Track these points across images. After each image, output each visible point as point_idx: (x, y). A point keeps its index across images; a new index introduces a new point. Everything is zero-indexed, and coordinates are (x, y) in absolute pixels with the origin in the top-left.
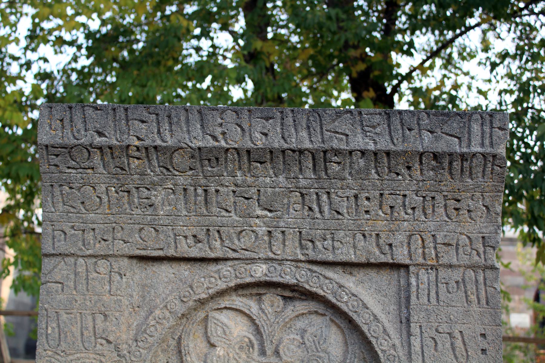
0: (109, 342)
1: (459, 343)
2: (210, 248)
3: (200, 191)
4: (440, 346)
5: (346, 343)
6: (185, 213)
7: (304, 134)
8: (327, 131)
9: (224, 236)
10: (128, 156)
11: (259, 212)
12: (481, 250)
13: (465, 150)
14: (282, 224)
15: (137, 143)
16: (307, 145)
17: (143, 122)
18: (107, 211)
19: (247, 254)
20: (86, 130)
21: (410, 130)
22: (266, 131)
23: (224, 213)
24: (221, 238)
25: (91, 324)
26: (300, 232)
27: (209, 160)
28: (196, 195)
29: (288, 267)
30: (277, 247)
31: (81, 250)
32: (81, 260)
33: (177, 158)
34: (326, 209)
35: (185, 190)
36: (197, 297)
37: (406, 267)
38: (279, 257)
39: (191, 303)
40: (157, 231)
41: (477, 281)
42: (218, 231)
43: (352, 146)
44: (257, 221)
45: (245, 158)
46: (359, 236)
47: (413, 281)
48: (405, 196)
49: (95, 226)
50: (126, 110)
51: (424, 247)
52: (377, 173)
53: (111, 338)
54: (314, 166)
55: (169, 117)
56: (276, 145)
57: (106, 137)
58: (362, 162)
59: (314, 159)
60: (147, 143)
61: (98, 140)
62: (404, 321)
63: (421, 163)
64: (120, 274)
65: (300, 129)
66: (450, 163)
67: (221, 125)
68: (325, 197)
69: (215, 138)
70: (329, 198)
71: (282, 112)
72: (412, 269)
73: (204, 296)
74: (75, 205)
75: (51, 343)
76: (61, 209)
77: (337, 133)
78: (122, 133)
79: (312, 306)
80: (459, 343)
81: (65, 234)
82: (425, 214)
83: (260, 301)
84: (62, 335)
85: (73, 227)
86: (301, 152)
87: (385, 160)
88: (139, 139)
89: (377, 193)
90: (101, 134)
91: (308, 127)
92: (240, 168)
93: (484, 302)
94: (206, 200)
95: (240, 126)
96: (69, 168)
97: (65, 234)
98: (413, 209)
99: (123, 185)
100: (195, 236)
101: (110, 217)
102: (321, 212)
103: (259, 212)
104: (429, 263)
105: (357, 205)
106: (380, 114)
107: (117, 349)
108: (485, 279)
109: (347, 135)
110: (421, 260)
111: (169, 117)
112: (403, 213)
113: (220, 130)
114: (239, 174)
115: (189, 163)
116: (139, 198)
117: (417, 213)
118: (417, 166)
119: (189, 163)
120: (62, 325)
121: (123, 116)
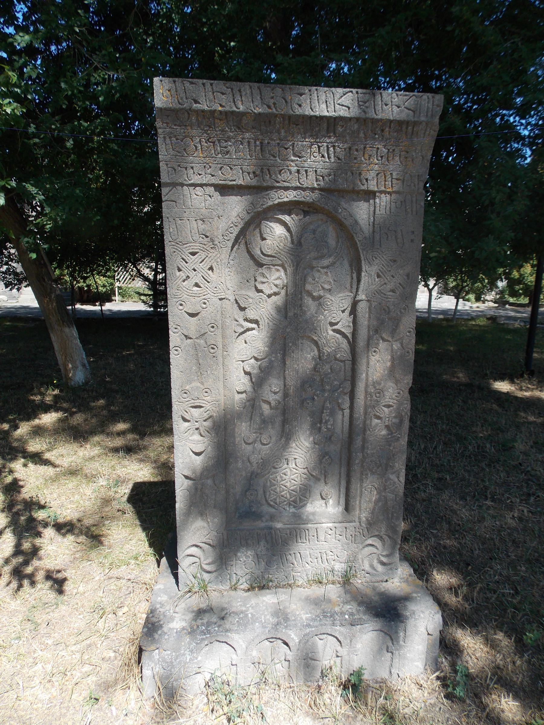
0: (207, 237)
1: (399, 235)
2: (264, 181)
3: (258, 143)
4: (390, 237)
5: (338, 237)
6: (249, 157)
7: (324, 106)
8: (339, 104)
9: (272, 172)
10: (214, 118)
11: (293, 158)
12: (416, 183)
13: (416, 119)
14: (306, 165)
15: (220, 109)
17: (223, 94)
18: (201, 155)
19: (286, 184)
20: (186, 98)
21: (386, 105)
22: (300, 103)
23: (272, 158)
24: (270, 174)
25: (195, 226)
26: (316, 171)
27: (265, 122)
28: (256, 146)
29: (307, 193)
30: (303, 179)
31: (185, 180)
32: (185, 187)
33: (245, 121)
34: (332, 156)
35: (249, 142)
36: (256, 210)
38: (304, 186)
39: (253, 214)
40: (231, 169)
41: (412, 201)
42: (268, 170)
44: (292, 163)
45: (287, 122)
46: (349, 173)
48: (378, 148)
49: (193, 165)
50: (211, 84)
51: (385, 181)
52: (364, 133)
53: (208, 235)
54: (328, 128)
55: (240, 91)
56: (307, 113)
57: (200, 103)
59: (328, 123)
60: (227, 109)
62: (371, 224)
63: (390, 127)
64: (210, 196)
65: (321, 103)
66: (407, 128)
67: (272, 98)
68: (332, 149)
69: (269, 107)
70: (334, 149)
71: (310, 91)
72: (377, 194)
73: (260, 209)
74: (179, 150)
75: (173, 237)
76: (172, 153)
77: (343, 105)
78: (211, 101)
79: (320, 216)
80: (399, 235)
81: (175, 170)
82: (388, 161)
84: (179, 233)
85: (179, 166)
87: (370, 124)
88: (221, 105)
89: (362, 146)
91: (326, 102)
92: (283, 128)
93: (414, 213)
94: (261, 149)
95: (285, 99)
96: (175, 125)
97: (175, 170)
98: (382, 157)
99: (210, 138)
100: (254, 173)
101: (203, 159)
102: (329, 158)
103: (293, 158)
104: (388, 190)
105: (350, 153)
106: (369, 94)
107: (212, 241)
108: (416, 200)
109: (349, 108)
110: (383, 188)
111: (240, 91)
112: (376, 160)
113: (272, 101)
114: (283, 131)
116: (221, 147)
117: (383, 160)
118: (387, 129)
120: (178, 227)
121: (210, 89)
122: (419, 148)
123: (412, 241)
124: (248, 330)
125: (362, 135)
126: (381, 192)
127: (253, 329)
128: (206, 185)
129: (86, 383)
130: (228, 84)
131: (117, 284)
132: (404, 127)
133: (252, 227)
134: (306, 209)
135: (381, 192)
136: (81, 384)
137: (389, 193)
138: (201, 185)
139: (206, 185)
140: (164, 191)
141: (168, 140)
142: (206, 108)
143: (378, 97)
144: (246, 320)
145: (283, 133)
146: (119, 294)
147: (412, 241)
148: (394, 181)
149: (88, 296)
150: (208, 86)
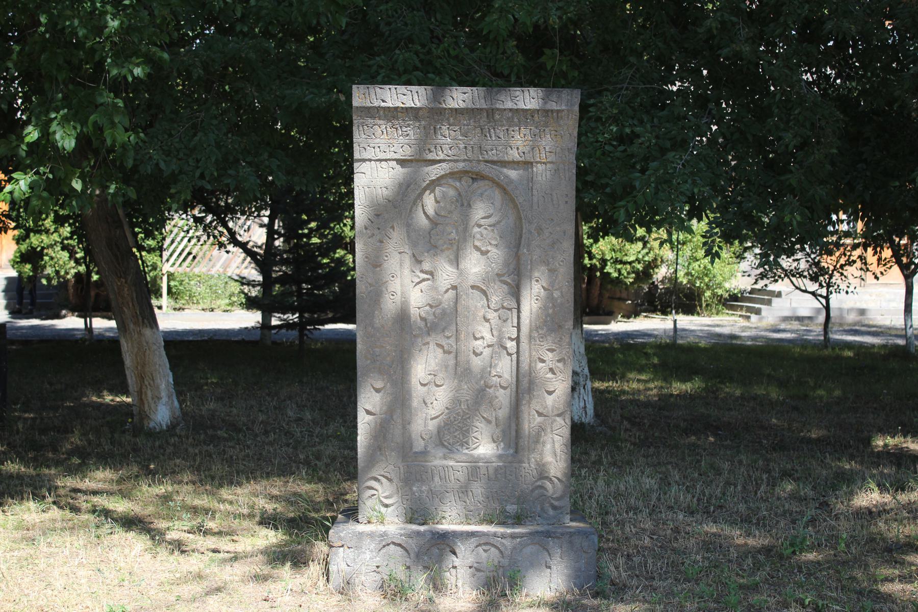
16: (484, 106)
33: (421, 113)
37: (532, 163)
43: (506, 107)
47: (535, 169)
58: (510, 114)
60: (408, 105)
61: (383, 104)
79: (487, 182)
80: (555, 198)
83: (460, 181)
86: (481, 109)
90: (383, 101)
110: (538, 160)
115: (427, 115)
119: (427, 115)
122: (566, 128)
123: (566, 202)
124: (424, 280)
125: (516, 120)
126: (537, 163)
127: (428, 279)
128: (390, 160)
129: (172, 427)
130: (409, 87)
131: (166, 268)
132: (550, 114)
133: (428, 192)
134: (474, 176)
135: (537, 163)
136: (165, 427)
137: (544, 163)
138: (386, 160)
139: (390, 160)
140: (356, 165)
141: (361, 128)
142: (391, 105)
143: (526, 93)
144: (422, 271)
145: (452, 120)
146: (170, 291)
147: (566, 202)
148: (548, 154)
149: (97, 295)
150: (393, 90)
